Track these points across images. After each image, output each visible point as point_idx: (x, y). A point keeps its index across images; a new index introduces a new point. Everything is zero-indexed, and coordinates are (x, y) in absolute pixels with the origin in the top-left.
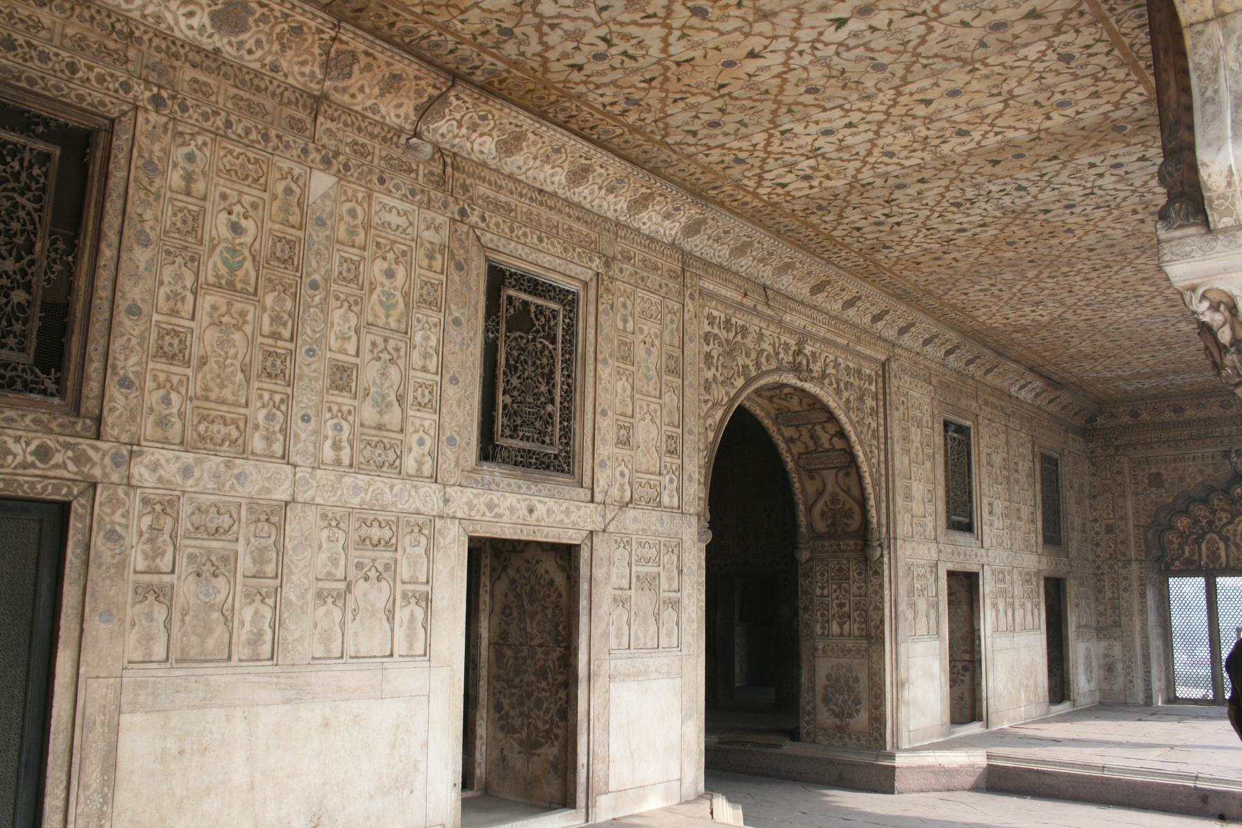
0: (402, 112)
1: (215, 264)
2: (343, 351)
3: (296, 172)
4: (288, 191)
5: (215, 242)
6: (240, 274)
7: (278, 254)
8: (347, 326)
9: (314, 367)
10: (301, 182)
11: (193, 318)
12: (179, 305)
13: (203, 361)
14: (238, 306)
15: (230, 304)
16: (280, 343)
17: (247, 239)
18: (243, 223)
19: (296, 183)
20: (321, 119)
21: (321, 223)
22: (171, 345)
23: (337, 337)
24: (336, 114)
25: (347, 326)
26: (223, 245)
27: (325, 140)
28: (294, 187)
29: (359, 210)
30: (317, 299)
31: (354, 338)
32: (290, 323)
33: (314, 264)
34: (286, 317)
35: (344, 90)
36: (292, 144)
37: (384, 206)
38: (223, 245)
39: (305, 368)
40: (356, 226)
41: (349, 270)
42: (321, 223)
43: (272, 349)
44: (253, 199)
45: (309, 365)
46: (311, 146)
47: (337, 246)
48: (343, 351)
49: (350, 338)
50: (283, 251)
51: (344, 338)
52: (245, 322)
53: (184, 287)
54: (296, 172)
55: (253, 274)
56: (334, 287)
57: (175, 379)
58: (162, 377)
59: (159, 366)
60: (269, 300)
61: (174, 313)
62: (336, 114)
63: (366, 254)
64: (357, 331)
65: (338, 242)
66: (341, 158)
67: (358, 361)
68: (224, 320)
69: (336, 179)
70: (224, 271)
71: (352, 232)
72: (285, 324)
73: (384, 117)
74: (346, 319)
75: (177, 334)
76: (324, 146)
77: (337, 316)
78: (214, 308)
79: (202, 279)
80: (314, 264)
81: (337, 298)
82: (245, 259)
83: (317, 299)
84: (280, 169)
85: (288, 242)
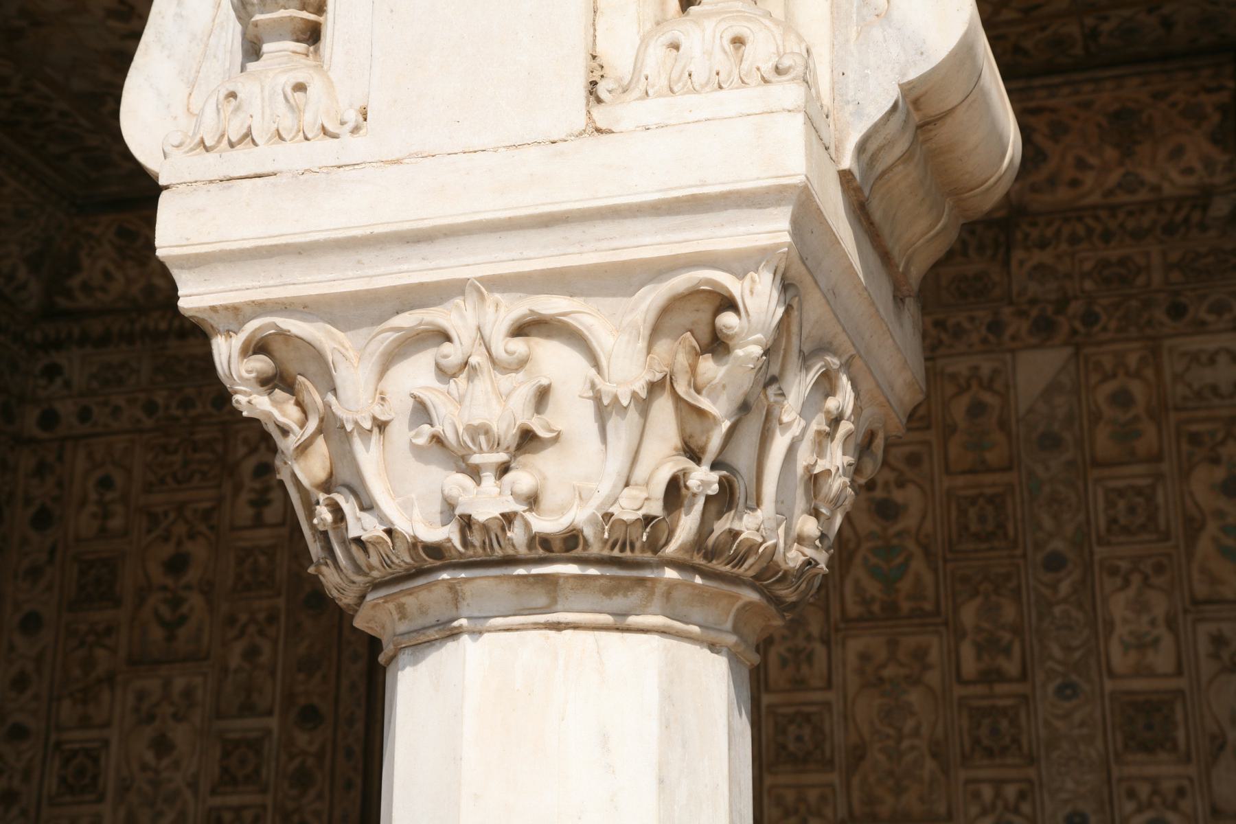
0: (1191, 158)
1: (857, 582)
2: (1143, 671)
3: (986, 367)
4: (977, 409)
5: (852, 545)
6: (905, 585)
7: (974, 527)
8: (1145, 619)
9: (1078, 717)
10: (998, 386)
11: (829, 685)
12: (805, 669)
13: (858, 754)
14: (909, 642)
15: (893, 644)
16: (1000, 688)
17: (909, 521)
18: (898, 496)
19: (989, 387)
20: (1018, 254)
21: (1050, 442)
22: (799, 739)
23: (1126, 647)
24: (1049, 232)
25: (1145, 619)
26: (866, 545)
27: (1033, 288)
28: (988, 398)
29: (1137, 389)
30: (1064, 588)
31: (1167, 641)
32: (1017, 648)
33: (1048, 523)
34: (1006, 636)
35: (1052, 182)
36: (967, 325)
37: (1194, 358)
38: (866, 545)
39: (1059, 724)
40: (1137, 418)
41: (1132, 510)
42: (1050, 442)
43: (985, 703)
44: (907, 449)
45: (1067, 716)
46: (1007, 311)
47: (1095, 473)
48: (1143, 671)
49: (1156, 642)
50: (982, 519)
51: (1142, 644)
52: (926, 667)
53: (809, 638)
54: (986, 367)
55: (928, 578)
56: (1100, 552)
57: (813, 795)
58: (790, 797)
59: (782, 779)
60: (968, 615)
61: (799, 684)
62: (1049, 232)
63: (1165, 467)
64: (1171, 623)
65: (1096, 463)
66: (1076, 307)
67: (1182, 683)
68: (887, 673)
69: (1067, 352)
70: (873, 588)
71: (1126, 434)
72: (1007, 651)
73: (1156, 189)
74: (1140, 606)
75: (807, 718)
76: (1033, 302)
77: (1119, 606)
78: (864, 657)
79: (835, 613)
80: (1048, 523)
81: (1114, 572)
82: (910, 556)
83: (1064, 588)
84: (953, 377)
85: (991, 500)
